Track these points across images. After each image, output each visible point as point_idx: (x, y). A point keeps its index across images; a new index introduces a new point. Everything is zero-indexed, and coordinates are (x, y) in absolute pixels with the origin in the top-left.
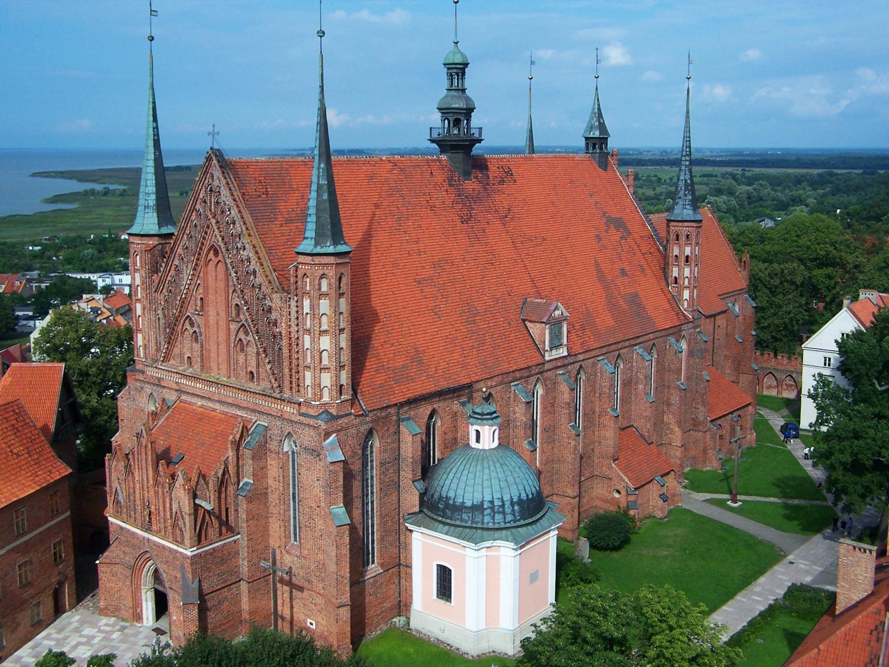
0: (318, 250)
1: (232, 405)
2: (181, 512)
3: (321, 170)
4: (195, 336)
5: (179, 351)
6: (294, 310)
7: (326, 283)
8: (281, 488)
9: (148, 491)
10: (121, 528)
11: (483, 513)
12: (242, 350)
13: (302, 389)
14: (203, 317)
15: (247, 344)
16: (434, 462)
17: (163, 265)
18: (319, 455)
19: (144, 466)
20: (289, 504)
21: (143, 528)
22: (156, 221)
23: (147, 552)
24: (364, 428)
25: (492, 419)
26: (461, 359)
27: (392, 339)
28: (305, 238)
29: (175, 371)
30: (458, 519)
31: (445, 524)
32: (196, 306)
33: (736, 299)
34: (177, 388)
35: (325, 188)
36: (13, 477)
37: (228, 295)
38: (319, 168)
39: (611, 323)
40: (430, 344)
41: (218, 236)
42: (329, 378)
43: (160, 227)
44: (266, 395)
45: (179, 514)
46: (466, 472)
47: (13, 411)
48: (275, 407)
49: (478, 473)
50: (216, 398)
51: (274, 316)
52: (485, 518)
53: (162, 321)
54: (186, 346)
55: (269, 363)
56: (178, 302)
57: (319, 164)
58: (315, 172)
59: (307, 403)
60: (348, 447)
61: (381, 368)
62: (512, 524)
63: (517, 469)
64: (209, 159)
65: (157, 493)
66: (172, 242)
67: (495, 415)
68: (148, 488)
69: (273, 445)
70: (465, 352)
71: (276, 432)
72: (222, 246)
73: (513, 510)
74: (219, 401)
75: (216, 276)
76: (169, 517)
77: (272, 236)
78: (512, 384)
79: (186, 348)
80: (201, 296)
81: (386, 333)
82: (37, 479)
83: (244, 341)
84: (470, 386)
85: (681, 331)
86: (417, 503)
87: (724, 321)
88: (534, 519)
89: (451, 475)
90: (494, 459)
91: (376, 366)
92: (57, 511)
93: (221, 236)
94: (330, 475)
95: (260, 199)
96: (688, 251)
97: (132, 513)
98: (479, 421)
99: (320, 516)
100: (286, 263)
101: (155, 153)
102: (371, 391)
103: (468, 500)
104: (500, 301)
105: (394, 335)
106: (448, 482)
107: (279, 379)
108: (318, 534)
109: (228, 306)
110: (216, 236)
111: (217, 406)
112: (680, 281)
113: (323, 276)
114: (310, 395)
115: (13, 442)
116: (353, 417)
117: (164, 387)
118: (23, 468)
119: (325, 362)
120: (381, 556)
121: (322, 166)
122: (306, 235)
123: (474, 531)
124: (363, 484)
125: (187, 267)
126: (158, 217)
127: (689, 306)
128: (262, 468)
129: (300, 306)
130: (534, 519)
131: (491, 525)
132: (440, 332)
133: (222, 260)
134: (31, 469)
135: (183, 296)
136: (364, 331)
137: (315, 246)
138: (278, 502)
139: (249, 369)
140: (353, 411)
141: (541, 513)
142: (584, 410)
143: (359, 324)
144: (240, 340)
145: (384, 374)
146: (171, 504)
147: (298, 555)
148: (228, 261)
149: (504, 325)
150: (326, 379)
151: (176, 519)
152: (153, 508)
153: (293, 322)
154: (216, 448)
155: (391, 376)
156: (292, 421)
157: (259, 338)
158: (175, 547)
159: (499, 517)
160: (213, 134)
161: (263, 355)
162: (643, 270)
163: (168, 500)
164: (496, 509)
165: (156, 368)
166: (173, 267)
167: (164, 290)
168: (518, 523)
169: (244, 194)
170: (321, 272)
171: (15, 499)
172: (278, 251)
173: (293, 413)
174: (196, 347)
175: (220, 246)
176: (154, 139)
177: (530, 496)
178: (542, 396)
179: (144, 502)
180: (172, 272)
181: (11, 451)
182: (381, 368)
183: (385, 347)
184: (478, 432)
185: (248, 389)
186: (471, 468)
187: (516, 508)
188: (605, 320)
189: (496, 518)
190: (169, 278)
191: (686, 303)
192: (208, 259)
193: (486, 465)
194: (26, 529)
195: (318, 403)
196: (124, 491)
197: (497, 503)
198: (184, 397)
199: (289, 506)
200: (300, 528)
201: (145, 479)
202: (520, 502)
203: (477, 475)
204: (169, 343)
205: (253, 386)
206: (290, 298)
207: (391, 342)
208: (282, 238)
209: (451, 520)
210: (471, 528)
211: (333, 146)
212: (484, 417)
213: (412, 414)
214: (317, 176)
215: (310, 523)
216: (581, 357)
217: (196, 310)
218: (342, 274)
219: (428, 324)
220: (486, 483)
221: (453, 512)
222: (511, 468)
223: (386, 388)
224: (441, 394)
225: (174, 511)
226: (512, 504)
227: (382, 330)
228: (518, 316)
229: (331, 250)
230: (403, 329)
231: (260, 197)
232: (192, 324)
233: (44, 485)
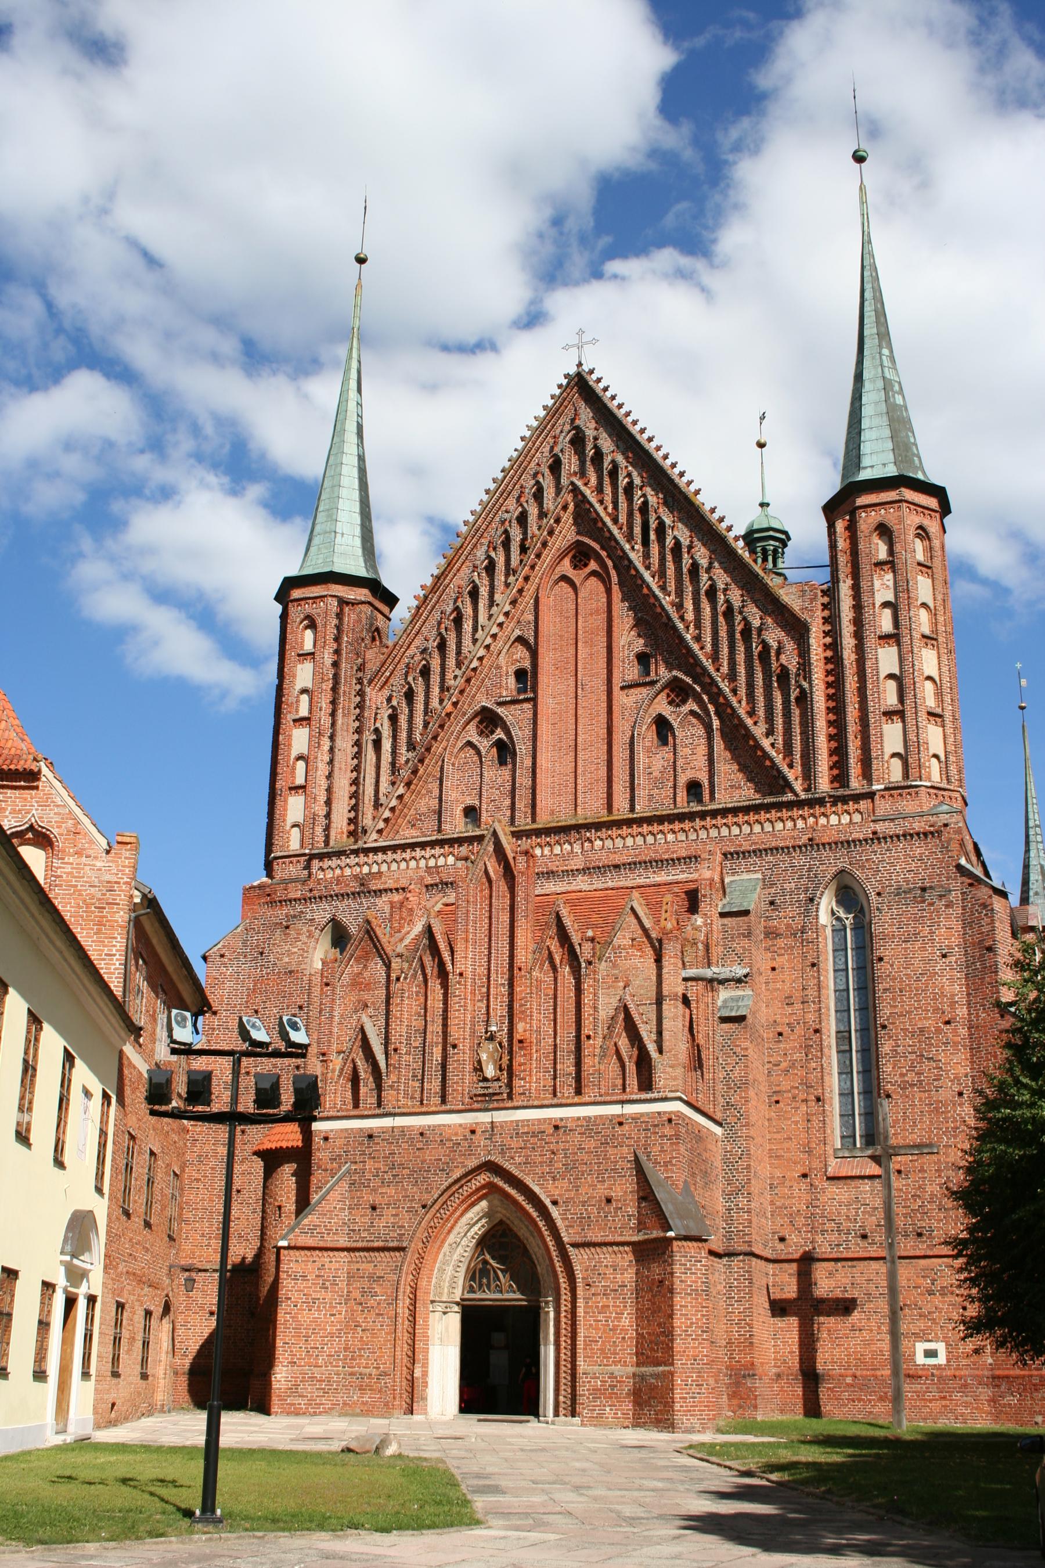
1: (632, 865)
50: (578, 863)
74: (585, 871)
108: (947, 1093)
111: (582, 883)
139: (683, 780)
204: (408, 784)
215: (919, 1074)
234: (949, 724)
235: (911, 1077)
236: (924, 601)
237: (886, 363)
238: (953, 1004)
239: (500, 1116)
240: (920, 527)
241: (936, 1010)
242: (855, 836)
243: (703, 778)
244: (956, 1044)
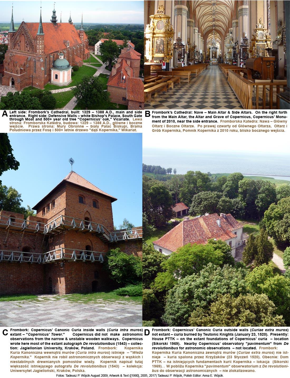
48: (32, 55)
54: (17, 47)
64: (22, 22)
69: (32, 60)
109: (25, 42)
129: (37, 42)
150: (40, 51)
180: (15, 37)
211: (43, 22)
214: (40, 25)
232: (18, 44)
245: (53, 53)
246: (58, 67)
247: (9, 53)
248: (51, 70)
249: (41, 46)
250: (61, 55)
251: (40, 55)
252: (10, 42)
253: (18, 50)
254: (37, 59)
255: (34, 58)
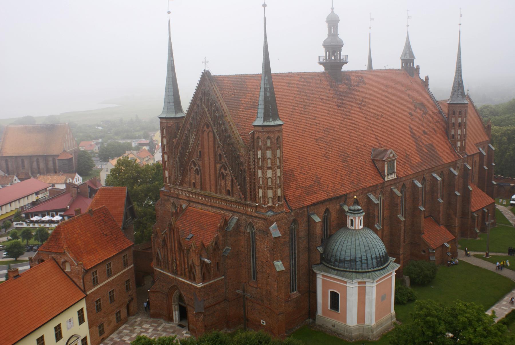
0: (266, 124)
2: (194, 265)
3: (266, 80)
4: (197, 172)
5: (188, 180)
6: (252, 157)
7: (270, 142)
8: (246, 252)
9: (175, 254)
10: (161, 273)
11: (356, 264)
12: (223, 178)
13: (257, 199)
14: (201, 162)
15: (226, 175)
16: (327, 237)
17: (179, 134)
18: (267, 234)
19: (173, 240)
20: (251, 259)
21: (173, 273)
22: (174, 111)
23: (175, 285)
24: (291, 219)
25: (359, 213)
26: (340, 181)
27: (304, 171)
28: (257, 117)
29: (186, 190)
30: (342, 267)
31: (335, 270)
32: (197, 155)
33: (484, 146)
34: (187, 199)
35: (268, 90)
36: (105, 247)
37: (215, 149)
38: (265, 79)
39: (419, 160)
40: (324, 173)
41: (209, 118)
42: (272, 192)
43: (176, 114)
44: (237, 202)
45: (193, 267)
46: (346, 242)
47: (103, 212)
48: (242, 209)
49: (353, 242)
50: (209, 204)
51: (242, 159)
52: (357, 266)
53: (178, 164)
54: (193, 177)
55: (238, 185)
56: (187, 153)
57: (265, 77)
58: (263, 82)
59: (260, 207)
60: (282, 230)
61: (298, 187)
62: (373, 270)
63: (374, 240)
65: (180, 255)
66: (183, 121)
67: (361, 211)
68: (175, 252)
69: (242, 228)
70: (342, 177)
71: (243, 222)
72: (212, 123)
73: (372, 262)
75: (208, 139)
76: (187, 267)
77: (238, 117)
78: (368, 194)
79: (192, 178)
80: (201, 150)
81: (300, 168)
82: (117, 247)
83: (224, 173)
84: (346, 195)
85: (456, 164)
86: (319, 259)
87: (478, 158)
88: (383, 266)
89: (338, 244)
90: (362, 234)
91: (296, 186)
92: (127, 264)
93: (210, 117)
94: (273, 244)
95: (231, 97)
96: (460, 120)
97: (167, 265)
98: (352, 215)
99: (268, 266)
100: (246, 131)
101: (172, 74)
102: (294, 199)
103: (347, 257)
104: (360, 150)
105: (305, 169)
106: (336, 247)
107: (245, 194)
110: (208, 118)
111: (210, 208)
112: (456, 137)
113: (269, 138)
114: (262, 202)
115: (104, 228)
116: (285, 213)
117: (180, 199)
118: (109, 242)
119: (270, 184)
120: (299, 288)
121: (267, 78)
122: (258, 116)
123: (351, 273)
124: (290, 249)
125: (192, 135)
126: (175, 108)
127: (460, 150)
128: (236, 241)
130: (383, 266)
131: (360, 271)
132: (328, 167)
133: (212, 130)
134: (113, 242)
135: (190, 150)
136: (289, 167)
137: (264, 121)
138: (244, 259)
139: (227, 188)
140: (285, 210)
141: (387, 264)
142: (405, 207)
143: (286, 164)
144: (222, 173)
145: (300, 190)
146: (188, 261)
147: (256, 287)
148: (215, 131)
149: (363, 162)
150: (270, 193)
151: (191, 268)
152: (178, 262)
153: (251, 163)
154: (211, 231)
155: (304, 191)
156: (252, 216)
157: (233, 172)
158: (190, 283)
159: (364, 266)
160: (205, 63)
161: (235, 181)
162: (435, 131)
163: (186, 258)
164: (363, 261)
165: (176, 189)
166: (184, 135)
167: (180, 147)
168: (375, 269)
169: (222, 95)
170: (267, 135)
171: (106, 258)
172: (242, 125)
173: (252, 212)
174: (198, 177)
175: (209, 123)
176: (172, 67)
177: (381, 254)
178: (383, 200)
179: (173, 260)
180: (184, 138)
181: (103, 233)
182: (298, 187)
183: (300, 175)
184: (352, 221)
185: (227, 199)
186: (349, 240)
187: (374, 261)
188: (416, 159)
189: (363, 266)
190: (182, 141)
191: (459, 149)
192: (204, 130)
193: (357, 238)
194: (113, 274)
195: (266, 206)
196: (162, 254)
197: (364, 258)
198: (191, 204)
199: (251, 261)
200: (257, 272)
201: (173, 248)
202: (376, 258)
203: (353, 244)
204: (182, 175)
205: (229, 198)
206: (250, 150)
207: (303, 173)
208: (243, 118)
209: (339, 267)
210: (349, 272)
212: (356, 212)
213: (316, 211)
215: (262, 270)
216: (404, 179)
217: (197, 158)
218: (278, 136)
219: (322, 163)
220: (358, 248)
221: (339, 263)
222: (370, 239)
223: (302, 197)
224: (330, 200)
225: (190, 264)
226: (372, 259)
227: (298, 167)
228: (369, 157)
229: (272, 123)
230: (310, 166)
231: (231, 95)
232: (195, 165)
233: (121, 251)
234: (274, 189)
235: (261, 270)
236: (269, 157)
237: (266, 82)
238: (268, 258)
239: (177, 278)
240: (269, 137)
241: (265, 258)
242: (253, 215)
243: (230, 189)
244: (268, 266)
245: (323, 202)
246: (340, 261)
247: (168, 200)
248: (315, 275)
249: (269, 174)
250: (355, 212)
251: (270, 208)
252: (168, 157)
253: (194, 191)
254: (259, 224)
255: (250, 220)
